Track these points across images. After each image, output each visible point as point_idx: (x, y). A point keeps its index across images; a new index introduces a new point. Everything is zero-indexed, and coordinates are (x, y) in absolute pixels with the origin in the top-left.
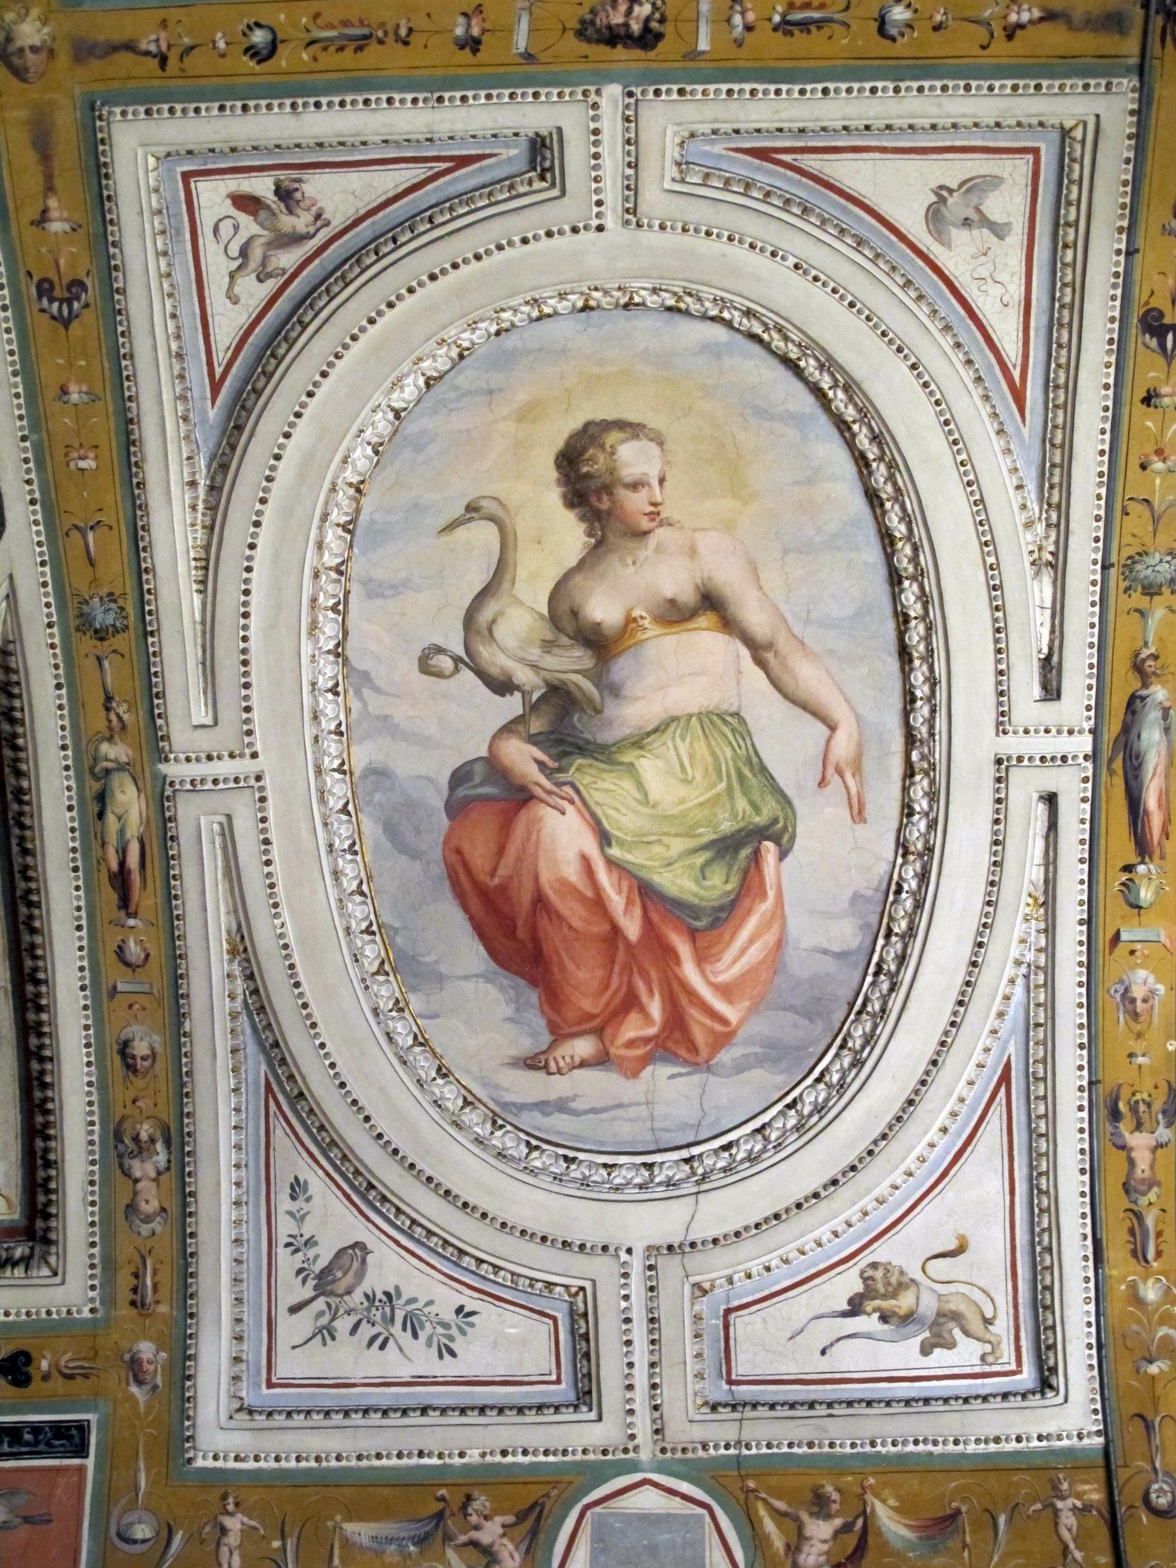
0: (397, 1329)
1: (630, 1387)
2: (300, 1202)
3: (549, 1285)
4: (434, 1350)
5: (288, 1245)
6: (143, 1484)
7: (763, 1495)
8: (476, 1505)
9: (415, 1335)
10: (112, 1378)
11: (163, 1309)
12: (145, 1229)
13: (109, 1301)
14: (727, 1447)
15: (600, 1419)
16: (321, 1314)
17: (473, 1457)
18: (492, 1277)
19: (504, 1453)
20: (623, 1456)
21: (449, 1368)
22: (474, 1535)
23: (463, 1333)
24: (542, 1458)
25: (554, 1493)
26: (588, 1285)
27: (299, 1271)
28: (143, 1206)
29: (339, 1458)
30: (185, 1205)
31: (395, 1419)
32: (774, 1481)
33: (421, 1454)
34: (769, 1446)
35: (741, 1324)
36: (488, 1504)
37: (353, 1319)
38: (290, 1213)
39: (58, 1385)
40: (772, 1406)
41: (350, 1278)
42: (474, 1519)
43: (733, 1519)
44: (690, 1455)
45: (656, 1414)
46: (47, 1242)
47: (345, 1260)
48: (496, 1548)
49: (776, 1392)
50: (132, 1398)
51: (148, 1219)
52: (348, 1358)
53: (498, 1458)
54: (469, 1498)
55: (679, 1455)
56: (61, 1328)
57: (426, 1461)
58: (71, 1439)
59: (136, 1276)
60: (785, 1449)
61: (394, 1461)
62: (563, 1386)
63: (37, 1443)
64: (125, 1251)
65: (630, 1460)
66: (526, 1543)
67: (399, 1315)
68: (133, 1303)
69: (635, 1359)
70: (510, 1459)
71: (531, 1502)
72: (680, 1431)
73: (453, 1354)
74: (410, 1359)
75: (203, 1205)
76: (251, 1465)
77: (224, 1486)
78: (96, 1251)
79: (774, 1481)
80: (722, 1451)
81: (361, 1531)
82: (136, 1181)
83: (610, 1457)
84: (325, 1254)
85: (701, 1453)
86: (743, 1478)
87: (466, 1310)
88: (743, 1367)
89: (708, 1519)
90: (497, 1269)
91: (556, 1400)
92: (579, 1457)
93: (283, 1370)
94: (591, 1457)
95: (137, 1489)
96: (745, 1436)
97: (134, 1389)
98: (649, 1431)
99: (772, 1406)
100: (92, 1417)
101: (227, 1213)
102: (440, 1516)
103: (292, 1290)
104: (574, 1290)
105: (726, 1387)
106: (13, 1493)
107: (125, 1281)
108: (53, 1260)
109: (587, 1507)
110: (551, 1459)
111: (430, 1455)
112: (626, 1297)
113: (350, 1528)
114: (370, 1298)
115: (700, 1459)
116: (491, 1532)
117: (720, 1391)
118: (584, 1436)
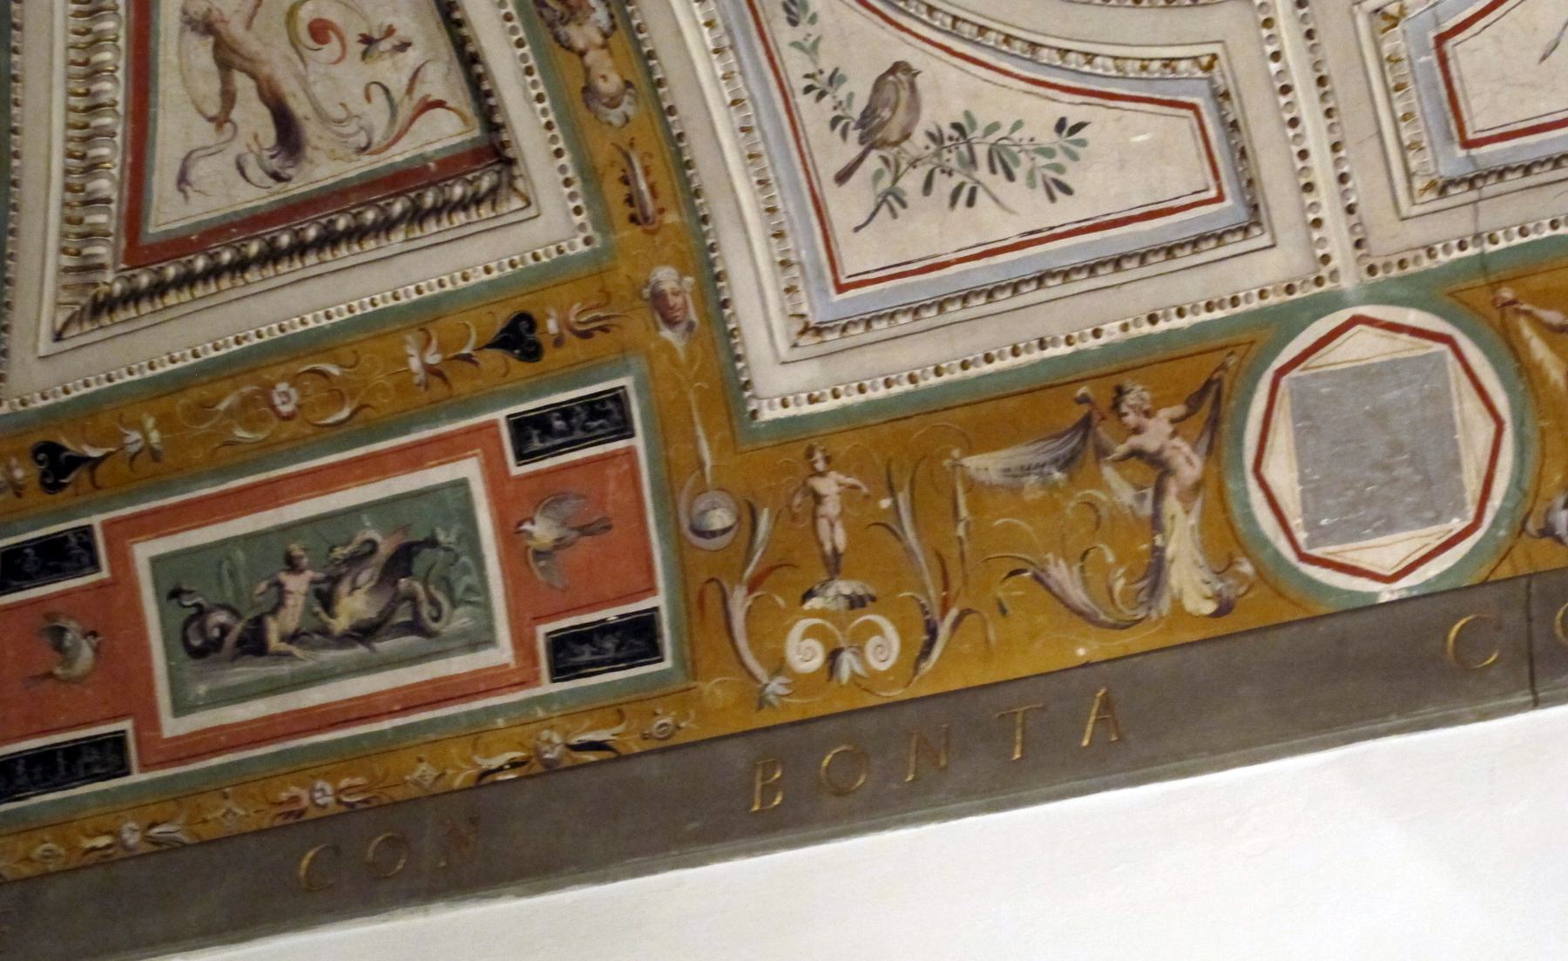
0: (982, 172)
1: (1309, 187)
2: (804, 27)
3: (1169, 62)
4: (1041, 192)
5: (808, 89)
6: (707, 456)
7: (1525, 307)
8: (1130, 399)
9: (1010, 177)
10: (636, 324)
11: (671, 218)
12: (615, 116)
13: (603, 222)
14: (1462, 246)
15: (1273, 246)
16: (878, 175)
17: (1112, 333)
18: (1087, 69)
19: (1153, 319)
20: (1317, 290)
21: (1066, 212)
22: (1135, 441)
23: (1074, 157)
24: (1205, 316)
25: (1232, 361)
26: (1216, 49)
27: (835, 122)
28: (603, 86)
29: (938, 372)
30: (650, 71)
31: (1004, 301)
32: (1538, 282)
33: (1042, 344)
34: (1523, 232)
35: (1467, 54)
36: (1146, 395)
37: (919, 174)
38: (795, 44)
39: (576, 349)
40: (1527, 170)
41: (901, 117)
42: (1131, 419)
43: (1486, 350)
44: (1411, 269)
45: (1354, 219)
46: (510, 162)
47: (888, 92)
48: (1167, 453)
49: (1540, 144)
50: (668, 347)
51: (614, 103)
52: (931, 229)
53: (1147, 329)
54: (1120, 392)
55: (1395, 272)
56: (554, 273)
57: (1050, 352)
58: (606, 416)
59: (625, 181)
60: (1548, 233)
61: (1010, 362)
62: (1229, 202)
63: (571, 429)
64: (603, 153)
65: (1329, 293)
66: (1205, 440)
67: (981, 152)
68: (633, 219)
69: (1309, 144)
70: (1162, 326)
71: (1203, 381)
72: (1390, 238)
73: (1067, 190)
74: (1012, 209)
75: (667, 65)
76: (829, 404)
77: (803, 440)
78: (565, 160)
79: (1538, 282)
80: (1456, 254)
81: (986, 465)
82: (582, 54)
83: (1297, 295)
84: (859, 90)
85: (1426, 263)
86: (1494, 286)
87: (1071, 123)
88: (1479, 121)
89: (1451, 357)
90: (1090, 57)
91: (1218, 226)
92: (1256, 304)
93: (851, 265)
94: (1272, 300)
95: (701, 465)
96: (1485, 225)
97: (666, 334)
98: (1349, 245)
99: (1527, 170)
100: (625, 381)
101: (706, 70)
102: (1086, 424)
103: (833, 152)
104: (1205, 61)
105: (1461, 153)
106: (559, 498)
107: (615, 193)
108: (520, 184)
109: (1282, 372)
110: (1218, 314)
111: (1054, 342)
112: (1276, 56)
113: (973, 463)
114: (936, 138)
115: (1427, 272)
116: (1156, 434)
117: (1455, 161)
118: (1257, 273)
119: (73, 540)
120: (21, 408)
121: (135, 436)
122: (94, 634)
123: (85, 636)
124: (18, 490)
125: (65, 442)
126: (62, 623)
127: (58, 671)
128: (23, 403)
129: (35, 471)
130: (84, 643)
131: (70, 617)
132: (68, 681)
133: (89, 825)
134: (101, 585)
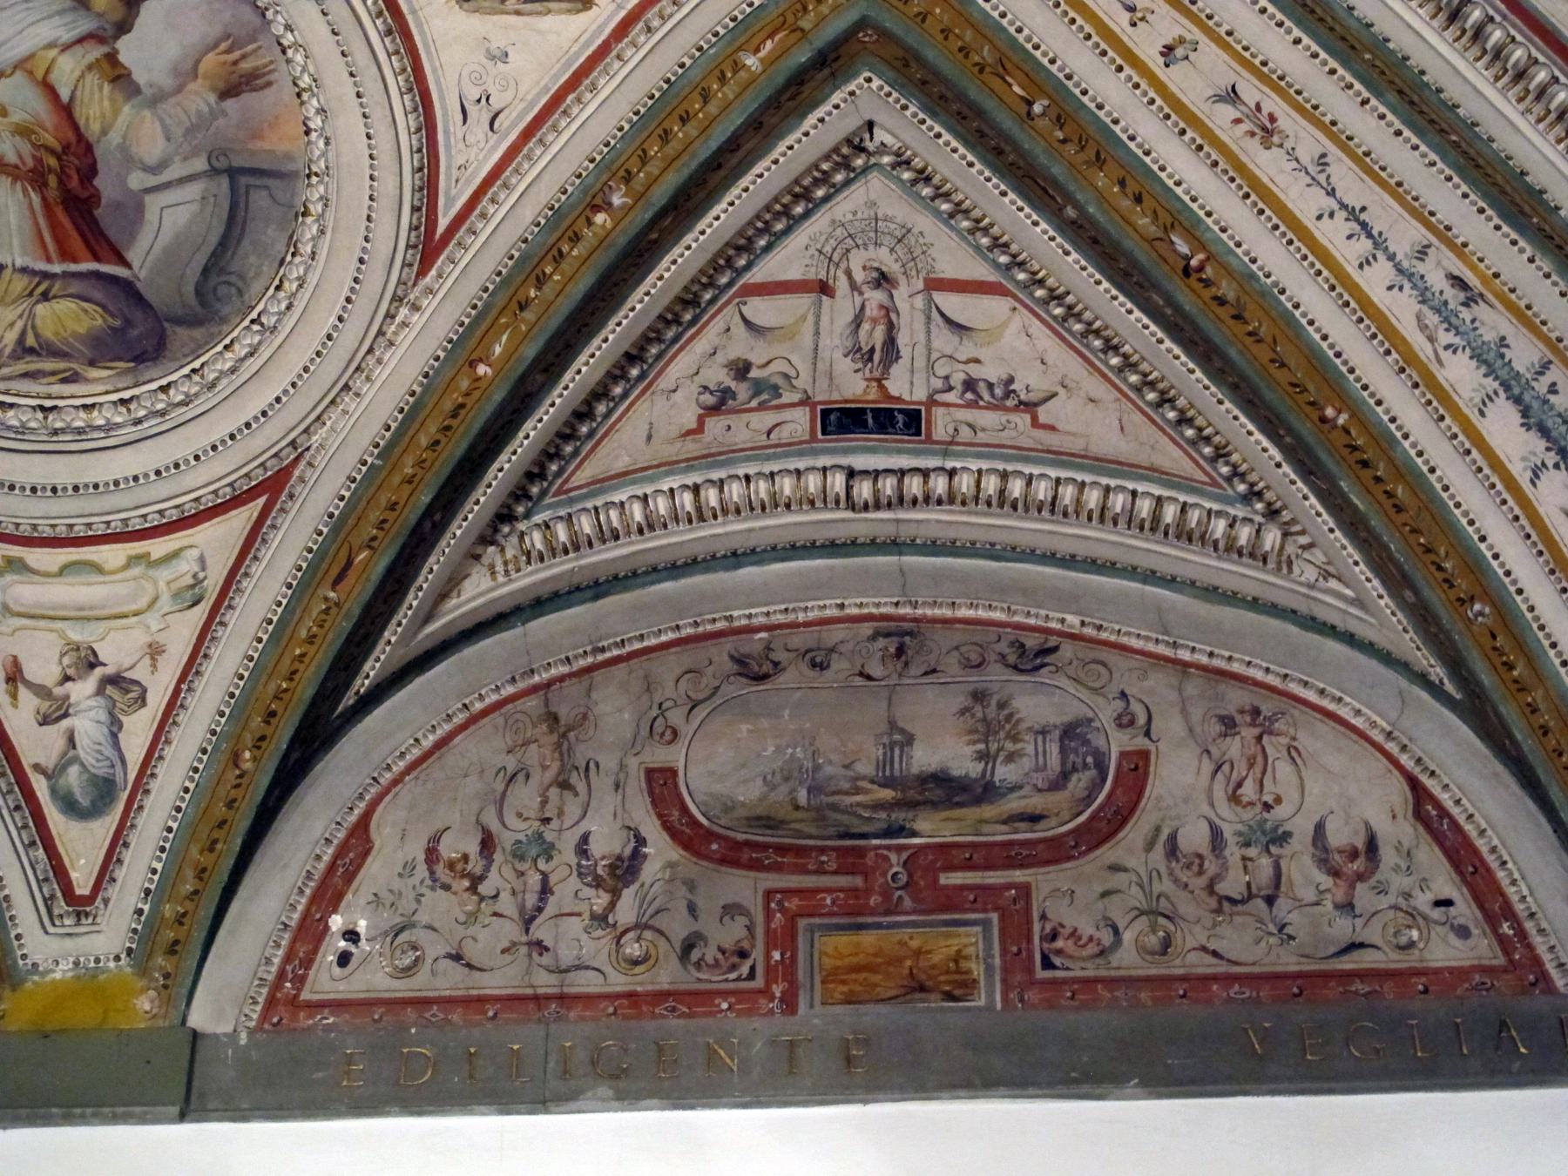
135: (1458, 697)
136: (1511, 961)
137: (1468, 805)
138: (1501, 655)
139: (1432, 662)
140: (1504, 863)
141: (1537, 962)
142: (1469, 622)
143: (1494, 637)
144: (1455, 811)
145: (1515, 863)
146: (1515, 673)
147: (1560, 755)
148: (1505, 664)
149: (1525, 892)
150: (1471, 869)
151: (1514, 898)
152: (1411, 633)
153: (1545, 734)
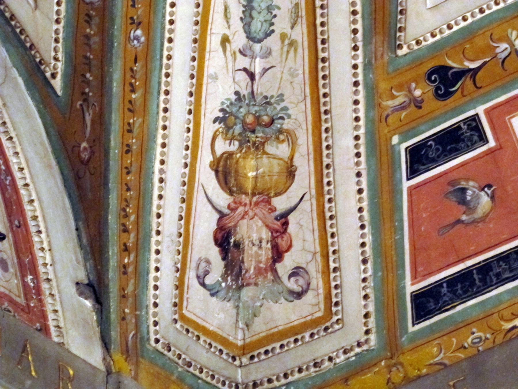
119: (465, 127)
120: (416, 47)
121: (504, 46)
122: (489, 186)
123: (483, 189)
124: (418, 104)
125: (450, 63)
126: (463, 184)
127: (464, 218)
128: (418, 43)
129: (430, 88)
130: (482, 193)
131: (467, 180)
132: (474, 222)
133: (507, 314)
134: (491, 151)
135: (60, 93)
136: (28, 305)
137: (28, 176)
138: (133, 77)
139: (60, 55)
140: (40, 232)
141: (44, 317)
142: (128, 39)
143: (136, 61)
144: (17, 175)
145: (48, 236)
146: (134, 96)
147: (128, 173)
148: (131, 85)
149: (48, 261)
150: (17, 223)
151: (40, 262)
152: (61, 26)
153: (127, 152)
